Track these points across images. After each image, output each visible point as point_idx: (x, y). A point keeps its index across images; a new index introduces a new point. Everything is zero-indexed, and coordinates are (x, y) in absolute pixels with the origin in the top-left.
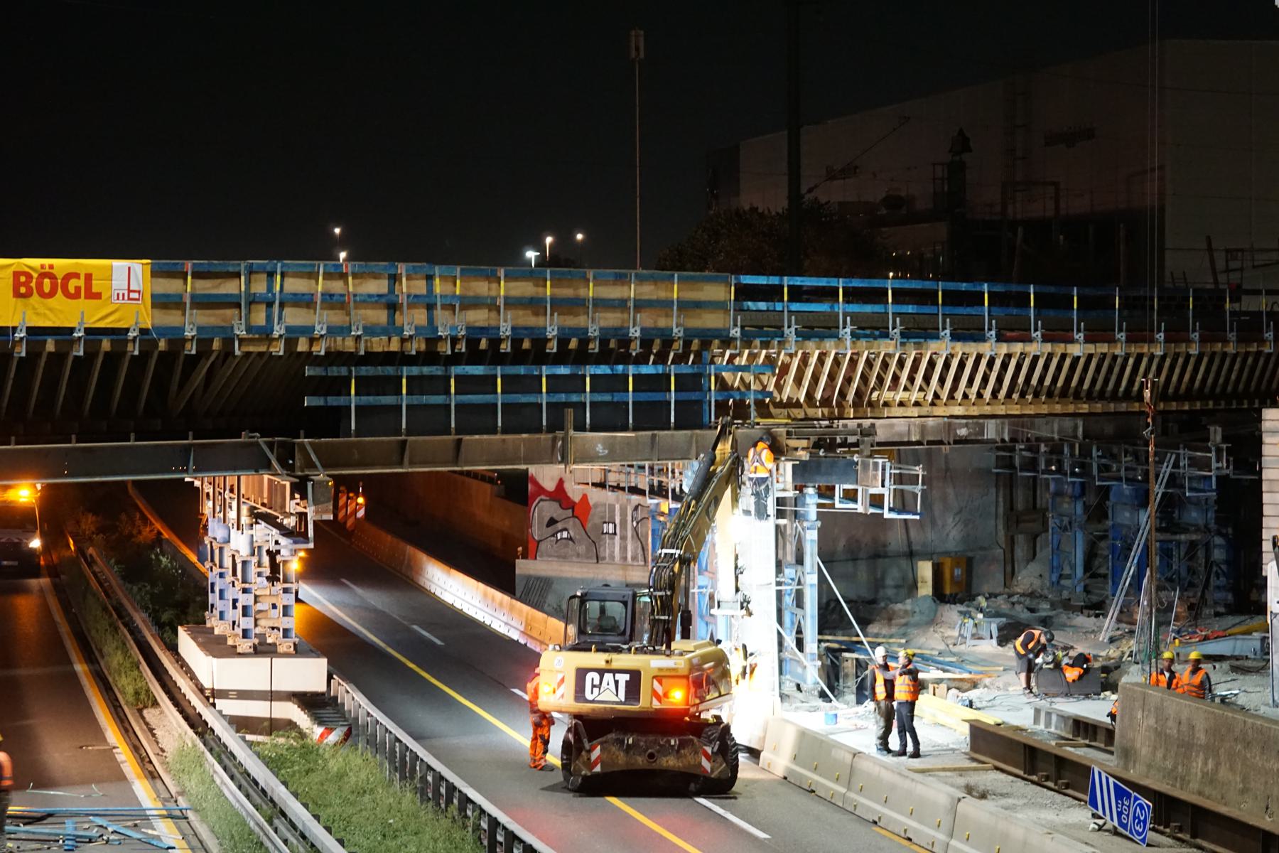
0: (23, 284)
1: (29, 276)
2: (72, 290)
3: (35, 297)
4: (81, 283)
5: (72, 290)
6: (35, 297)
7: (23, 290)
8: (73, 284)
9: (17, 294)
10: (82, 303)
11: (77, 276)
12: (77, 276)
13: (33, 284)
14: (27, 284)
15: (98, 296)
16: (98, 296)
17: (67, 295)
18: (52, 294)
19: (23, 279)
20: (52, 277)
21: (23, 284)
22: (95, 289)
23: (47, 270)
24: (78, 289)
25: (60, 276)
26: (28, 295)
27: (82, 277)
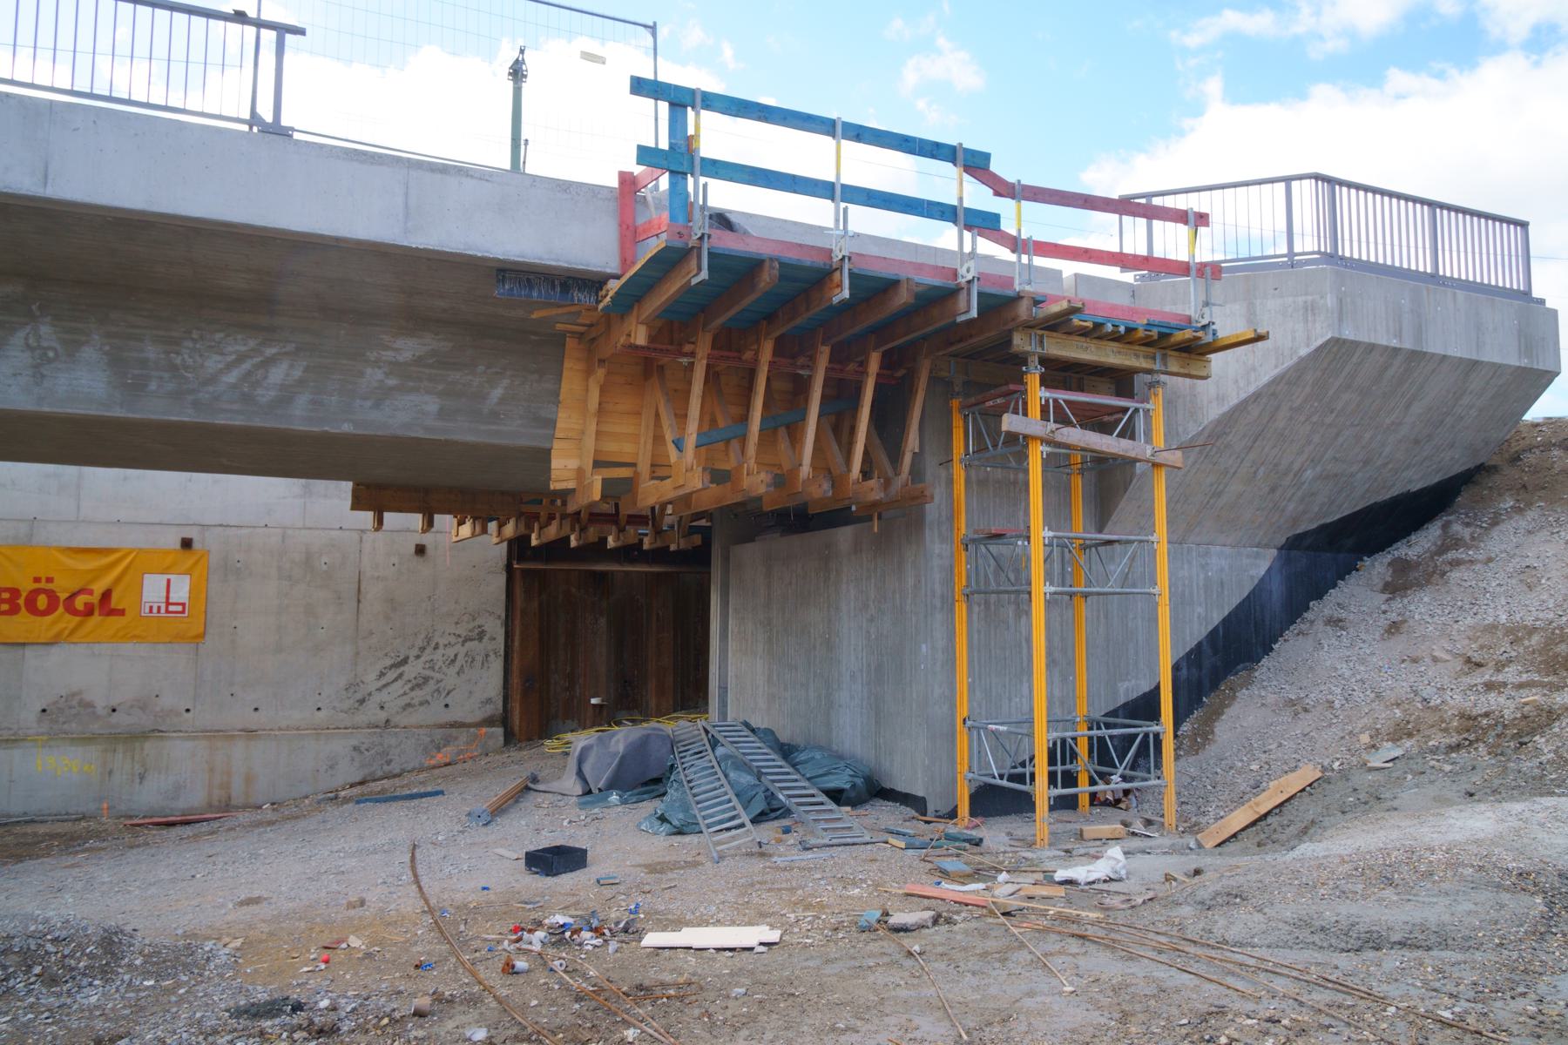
1: (15, 593)
8: (80, 603)
10: (96, 618)
13: (21, 601)
15: (121, 612)
16: (121, 612)
17: (75, 612)
20: (52, 595)
23: (43, 585)
25: (63, 596)
26: (14, 610)
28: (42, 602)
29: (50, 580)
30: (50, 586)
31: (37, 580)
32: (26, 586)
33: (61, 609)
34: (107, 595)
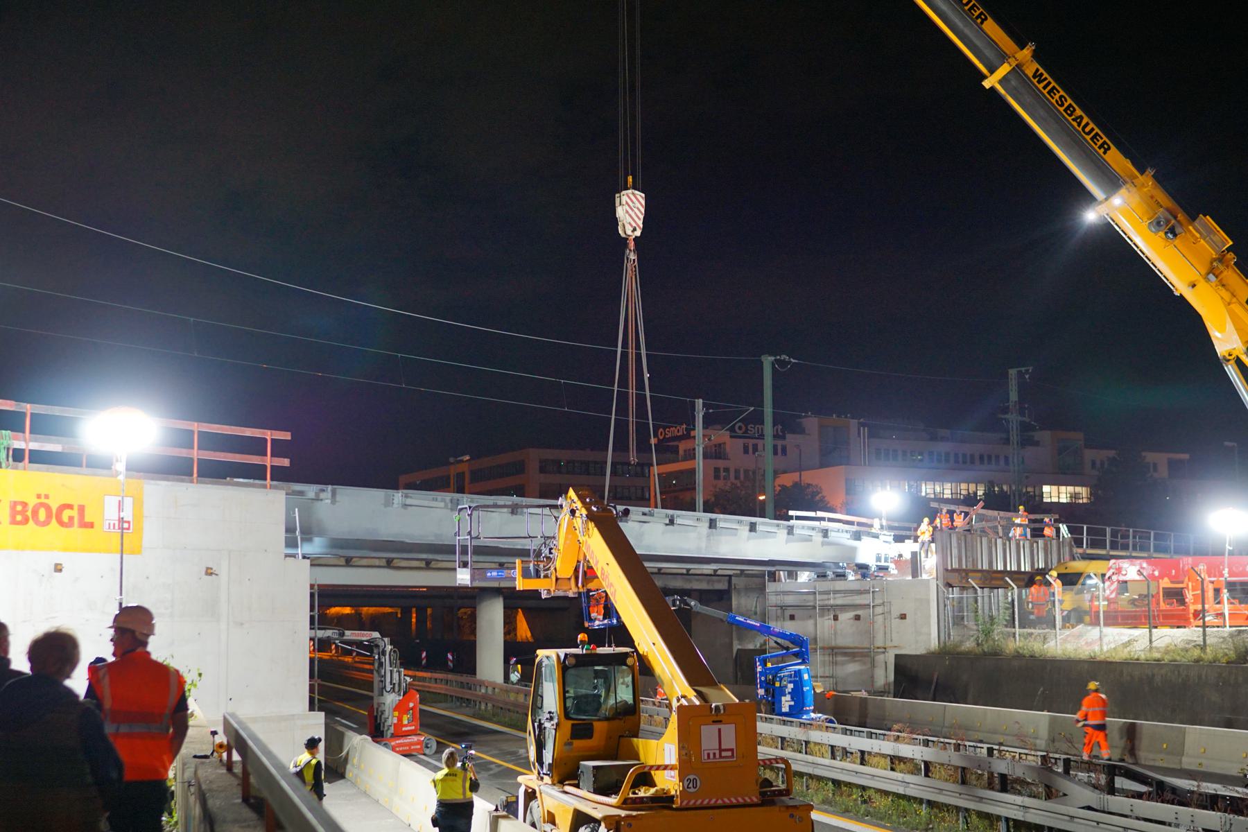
0: (19, 513)
1: (25, 505)
2: (65, 519)
3: (31, 521)
4: (74, 513)
5: (65, 519)
6: (31, 521)
7: (19, 518)
8: (66, 515)
9: (13, 522)
10: (76, 530)
11: (70, 507)
12: (70, 507)
13: (29, 514)
14: (23, 512)
15: (91, 525)
16: (91, 525)
17: (61, 523)
18: (46, 523)
19: (19, 508)
20: (48, 508)
21: (19, 513)
22: (87, 519)
23: (43, 500)
24: (71, 518)
26: (25, 521)
27: (76, 508)
28: (42, 514)
29: (47, 497)
30: (46, 501)
31: (39, 496)
32: (32, 501)
33: (54, 521)
34: (82, 509)
